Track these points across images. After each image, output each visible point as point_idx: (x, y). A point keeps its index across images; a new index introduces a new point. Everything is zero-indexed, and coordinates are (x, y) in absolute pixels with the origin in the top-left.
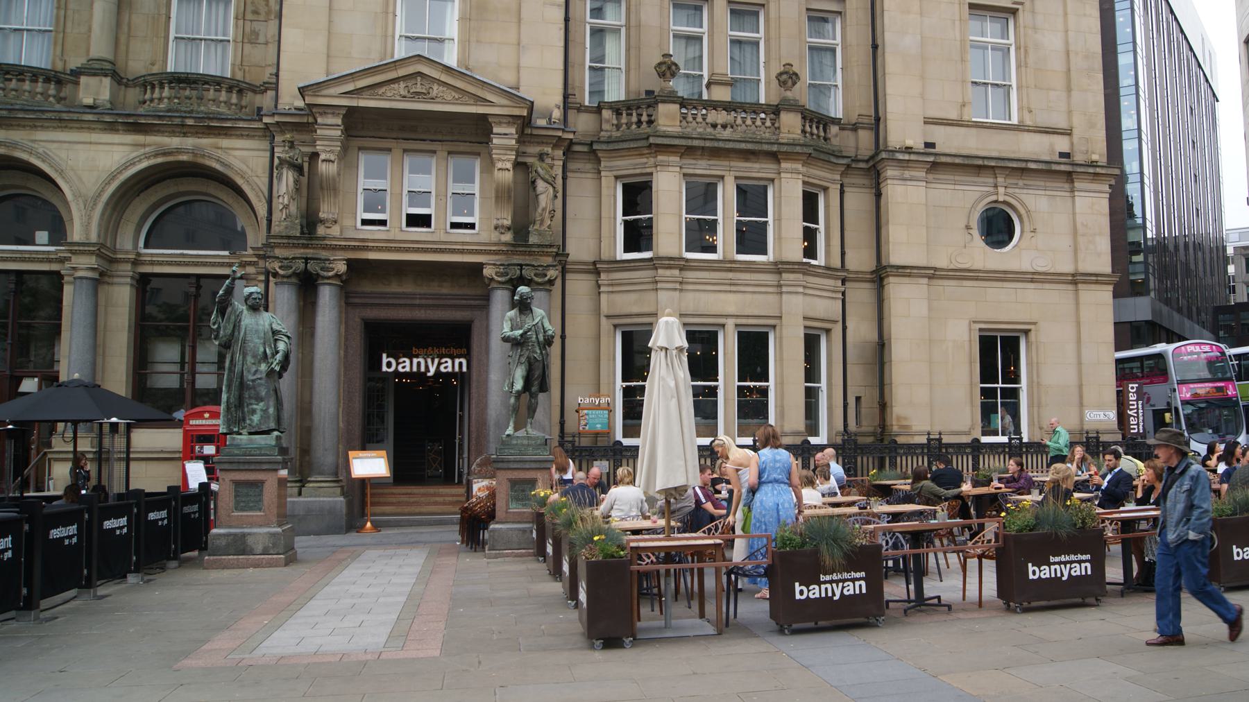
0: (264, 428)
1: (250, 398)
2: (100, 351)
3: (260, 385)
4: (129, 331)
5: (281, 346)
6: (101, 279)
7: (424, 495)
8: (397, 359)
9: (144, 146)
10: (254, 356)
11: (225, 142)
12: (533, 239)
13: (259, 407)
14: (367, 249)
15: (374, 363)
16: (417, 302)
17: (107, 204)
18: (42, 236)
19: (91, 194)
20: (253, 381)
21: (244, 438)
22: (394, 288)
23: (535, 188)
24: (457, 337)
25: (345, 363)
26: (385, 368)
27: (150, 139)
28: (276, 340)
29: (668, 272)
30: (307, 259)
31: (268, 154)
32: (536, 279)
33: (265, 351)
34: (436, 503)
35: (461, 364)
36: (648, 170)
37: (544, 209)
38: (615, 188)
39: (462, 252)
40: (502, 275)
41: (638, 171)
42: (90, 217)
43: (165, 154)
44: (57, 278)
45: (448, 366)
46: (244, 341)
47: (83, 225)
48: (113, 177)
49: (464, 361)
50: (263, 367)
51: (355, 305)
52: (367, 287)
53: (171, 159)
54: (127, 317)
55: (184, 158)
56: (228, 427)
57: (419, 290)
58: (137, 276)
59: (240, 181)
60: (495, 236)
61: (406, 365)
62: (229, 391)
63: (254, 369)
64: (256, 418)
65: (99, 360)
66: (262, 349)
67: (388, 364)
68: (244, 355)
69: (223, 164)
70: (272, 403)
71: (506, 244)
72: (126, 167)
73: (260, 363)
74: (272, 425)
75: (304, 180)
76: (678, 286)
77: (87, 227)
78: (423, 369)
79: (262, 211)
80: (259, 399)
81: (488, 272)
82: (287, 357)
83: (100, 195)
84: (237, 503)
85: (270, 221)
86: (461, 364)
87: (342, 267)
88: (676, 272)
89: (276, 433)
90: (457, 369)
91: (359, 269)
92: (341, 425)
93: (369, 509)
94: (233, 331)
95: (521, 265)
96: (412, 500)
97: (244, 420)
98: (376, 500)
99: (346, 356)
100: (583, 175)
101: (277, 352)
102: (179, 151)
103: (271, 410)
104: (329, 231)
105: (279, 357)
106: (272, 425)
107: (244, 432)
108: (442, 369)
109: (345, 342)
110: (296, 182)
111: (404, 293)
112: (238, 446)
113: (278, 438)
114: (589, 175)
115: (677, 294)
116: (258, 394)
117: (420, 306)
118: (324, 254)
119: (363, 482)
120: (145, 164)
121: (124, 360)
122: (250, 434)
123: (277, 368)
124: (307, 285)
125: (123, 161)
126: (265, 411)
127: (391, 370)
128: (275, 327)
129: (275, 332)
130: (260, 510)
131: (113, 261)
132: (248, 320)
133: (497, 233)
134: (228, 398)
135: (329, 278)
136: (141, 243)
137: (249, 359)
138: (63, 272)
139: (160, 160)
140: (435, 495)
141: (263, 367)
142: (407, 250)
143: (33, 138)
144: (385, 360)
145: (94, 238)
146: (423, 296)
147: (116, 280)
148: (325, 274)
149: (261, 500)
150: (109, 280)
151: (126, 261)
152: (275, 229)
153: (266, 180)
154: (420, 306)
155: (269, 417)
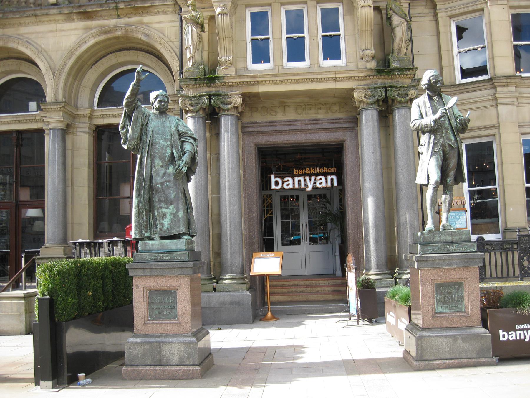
0: (175, 232)
1: (160, 201)
2: (69, 183)
3: (168, 188)
4: (89, 167)
5: (188, 147)
6: (66, 131)
7: (307, 286)
8: (282, 178)
9: (91, 28)
10: (161, 159)
11: (147, 19)
12: (395, 65)
13: (169, 210)
14: (256, 83)
15: (265, 184)
16: (299, 127)
17: (69, 74)
18: (33, 105)
19: (58, 67)
20: (162, 184)
21: (155, 244)
22: (280, 117)
23: (390, 24)
24: (330, 157)
25: (244, 180)
26: (273, 187)
27: (96, 23)
28: (183, 142)
29: (505, 89)
30: (210, 96)
31: (178, 24)
32: (399, 99)
33: (172, 153)
34: (318, 292)
35: (332, 180)
36: (479, 7)
37: (401, 39)
38: (450, 26)
39: (335, 80)
40: (370, 97)
41: (470, 9)
42: (57, 85)
43: (106, 32)
44: (40, 132)
45: (322, 182)
46: (151, 144)
47: (52, 89)
48: (71, 53)
49: (335, 178)
50: (171, 169)
51: (250, 134)
52: (258, 117)
53: (110, 36)
54: (87, 157)
55: (119, 33)
56: (141, 232)
57: (299, 117)
58: (94, 128)
59: (159, 47)
60: (362, 64)
61: (289, 183)
62: (139, 195)
63: (162, 171)
64: (166, 222)
65: (69, 189)
66: (169, 151)
67: (276, 183)
68: (152, 159)
69: (146, 35)
70: (181, 206)
71: (371, 70)
72: (80, 45)
73: (167, 166)
74: (183, 229)
75: (205, 35)
76: (515, 100)
77: (56, 91)
78: (303, 186)
79: (175, 66)
80: (169, 202)
81: (357, 95)
82: (193, 159)
83: (63, 68)
84: (152, 310)
85: (181, 72)
86: (332, 180)
87: (237, 100)
88: (512, 89)
89: (186, 237)
90: (329, 184)
91: (251, 101)
92: (244, 231)
93: (269, 298)
94: (141, 134)
95: (386, 88)
96: (299, 290)
97: (155, 224)
98: (276, 290)
99: (244, 175)
100: (422, 19)
101: (184, 154)
102: (115, 28)
103: (181, 214)
104: (226, 72)
105: (185, 158)
106: (183, 229)
107: (156, 236)
108: (318, 185)
109: (242, 164)
110: (199, 36)
111: (287, 121)
112: (150, 252)
113: (189, 243)
114: (427, 19)
115: (515, 107)
116: (167, 196)
117: (301, 131)
118: (222, 90)
119: (263, 278)
120: (92, 42)
121: (86, 189)
122: (162, 238)
123: (185, 170)
124: (211, 116)
125: (78, 41)
126: (175, 215)
127: (278, 188)
128: (181, 129)
129: (181, 135)
130: (175, 317)
131: (74, 117)
132: (154, 124)
133: (363, 62)
134: (139, 203)
135: (228, 110)
136: (96, 103)
137: (158, 162)
138: (44, 128)
139: (102, 37)
140: (316, 286)
141: (171, 169)
142: (290, 82)
143: (19, 32)
144: (273, 179)
145: (60, 98)
146: (304, 122)
147: (79, 130)
148: (226, 107)
149: (174, 308)
150: (75, 130)
151: (84, 115)
152: (185, 75)
153: (178, 44)
154: (301, 131)
155: (179, 221)
